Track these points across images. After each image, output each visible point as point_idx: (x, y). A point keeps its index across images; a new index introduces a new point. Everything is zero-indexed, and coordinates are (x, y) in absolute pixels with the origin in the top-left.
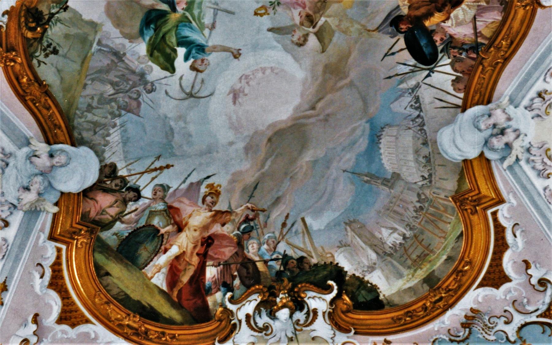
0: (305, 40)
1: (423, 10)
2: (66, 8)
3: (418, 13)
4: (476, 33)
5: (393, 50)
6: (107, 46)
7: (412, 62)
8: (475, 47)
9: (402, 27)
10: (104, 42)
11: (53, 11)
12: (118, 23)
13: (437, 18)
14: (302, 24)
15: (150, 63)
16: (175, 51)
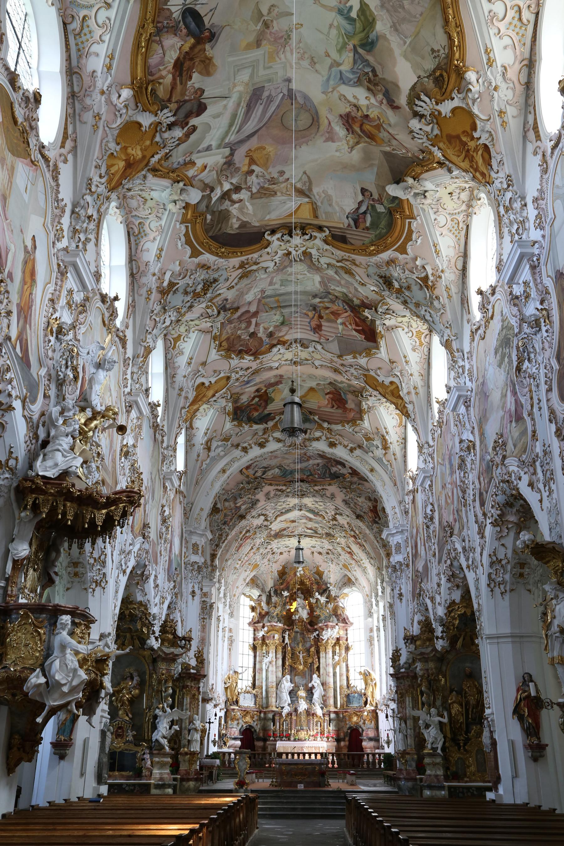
0: (269, 10)
1: (196, 50)
2: (419, 77)
3: (199, 47)
4: (160, 43)
5: (211, 13)
6: (401, 38)
7: (198, 8)
8: (159, 32)
9: (207, 34)
10: (402, 42)
11: (426, 79)
12: (391, 50)
13: (186, 48)
14: (272, 21)
15: (376, 13)
16: (358, 16)
